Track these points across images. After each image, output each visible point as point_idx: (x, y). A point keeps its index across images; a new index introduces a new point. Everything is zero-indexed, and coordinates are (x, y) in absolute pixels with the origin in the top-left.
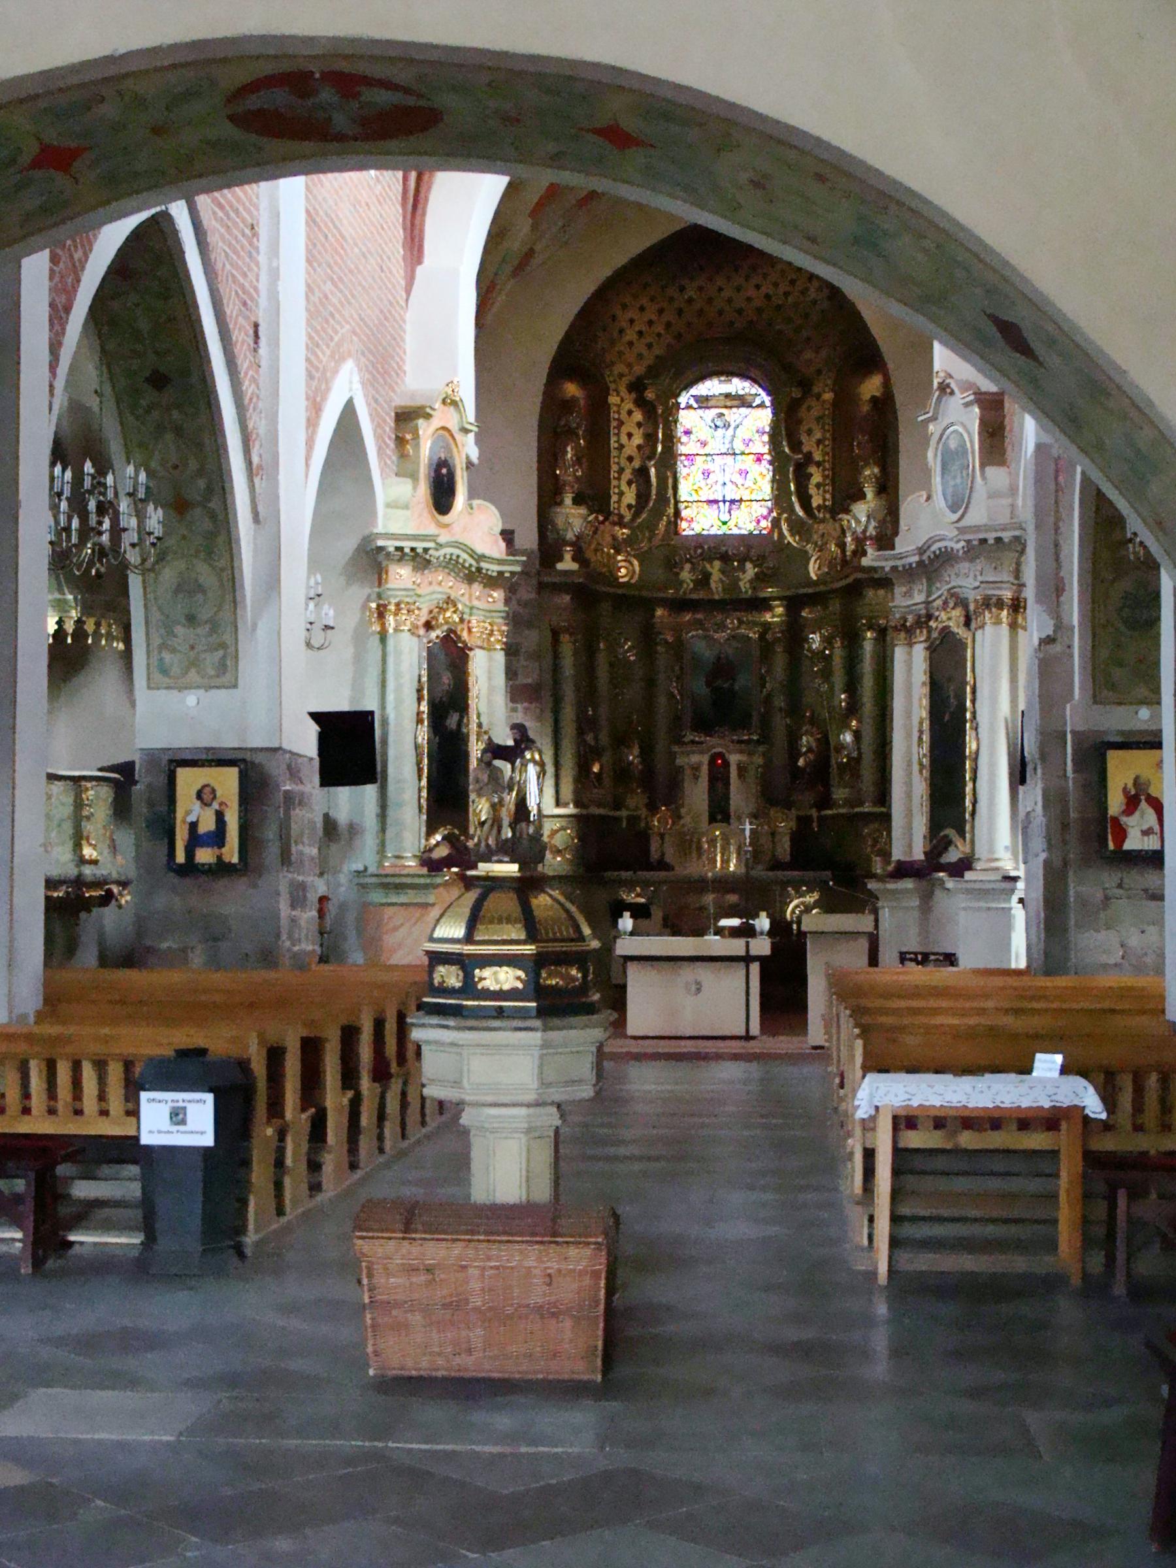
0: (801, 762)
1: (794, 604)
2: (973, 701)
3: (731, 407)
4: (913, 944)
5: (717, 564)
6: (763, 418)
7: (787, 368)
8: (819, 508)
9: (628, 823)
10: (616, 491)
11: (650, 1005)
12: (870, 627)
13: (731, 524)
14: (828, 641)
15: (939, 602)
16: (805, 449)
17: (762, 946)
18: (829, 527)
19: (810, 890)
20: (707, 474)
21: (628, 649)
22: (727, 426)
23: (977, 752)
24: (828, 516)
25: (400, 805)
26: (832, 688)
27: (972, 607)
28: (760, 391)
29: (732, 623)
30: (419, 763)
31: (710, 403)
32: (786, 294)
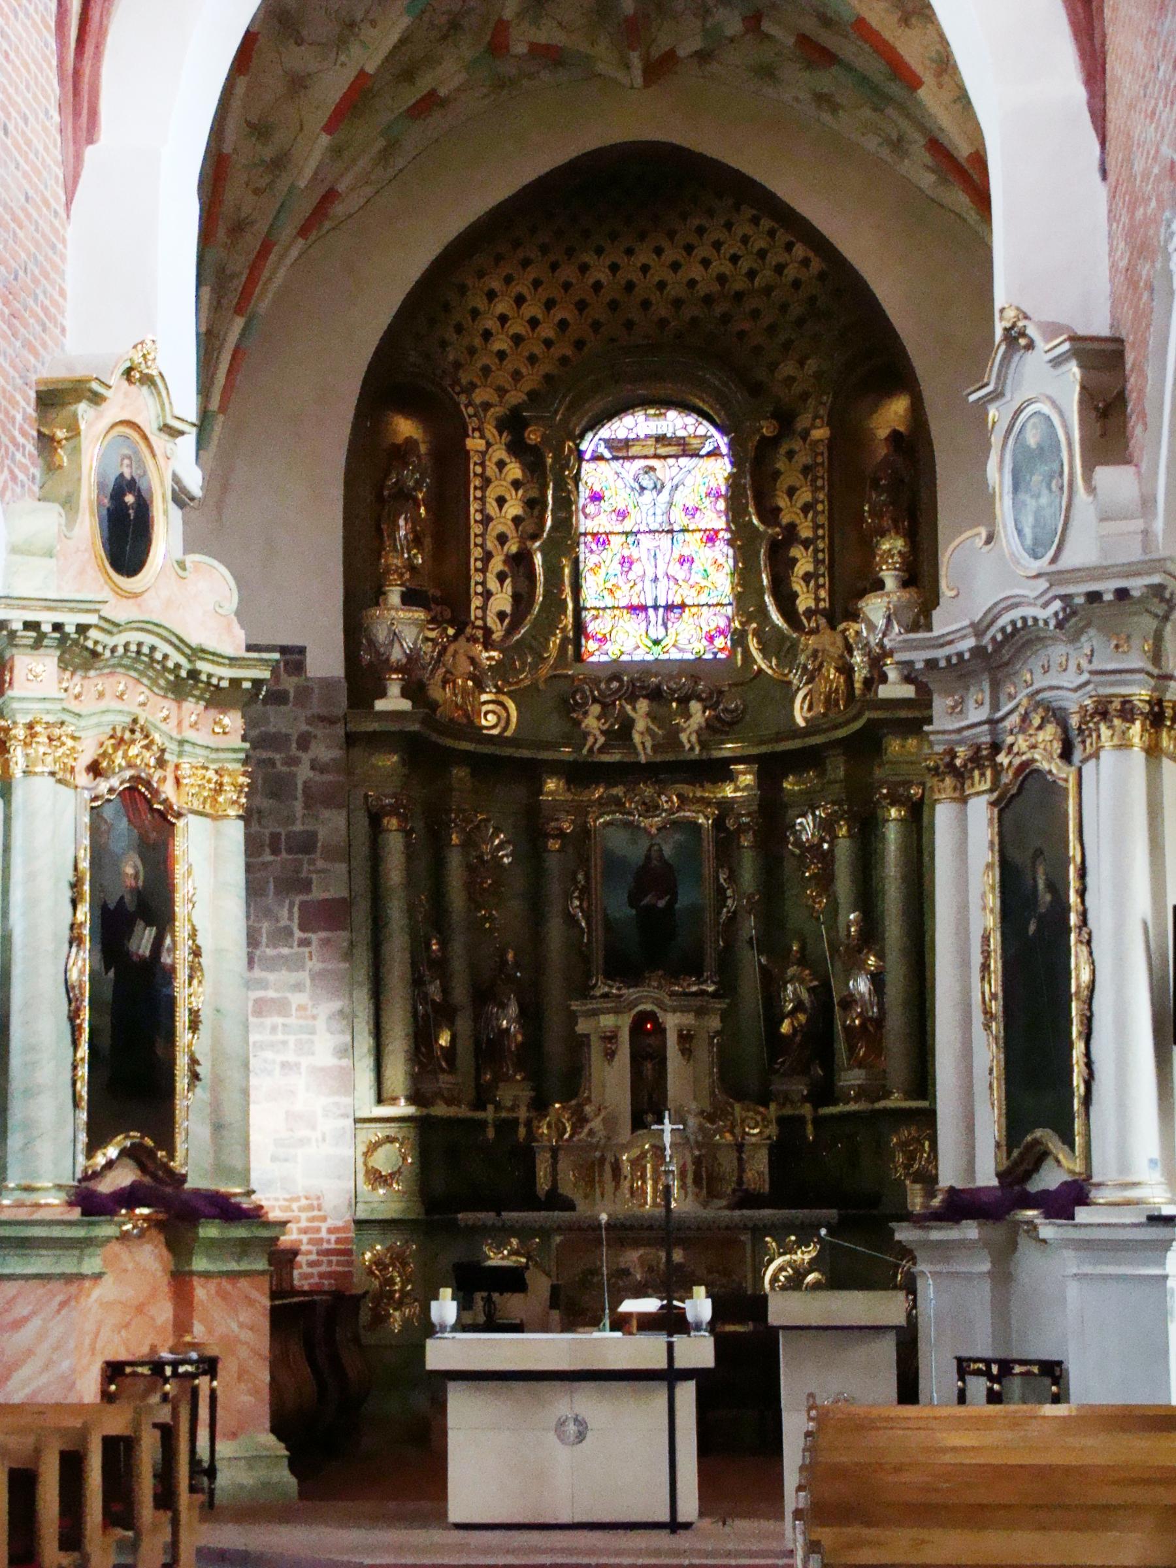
0: (785, 1027)
1: (771, 769)
2: (1082, 893)
3: (665, 457)
4: (982, 1346)
5: (643, 705)
6: (719, 471)
7: (756, 390)
8: (809, 613)
9: (497, 1132)
10: (479, 589)
11: (488, 1461)
13: (668, 641)
14: (827, 826)
15: (1015, 719)
16: (785, 519)
17: (698, 1351)
18: (827, 641)
19: (802, 1242)
20: (627, 562)
21: (501, 847)
22: (658, 488)
23: (1092, 987)
24: (823, 622)
25: (30, 1093)
27: (1074, 721)
28: (712, 431)
29: (670, 800)
30: (73, 1016)
31: (633, 451)
32: (752, 274)
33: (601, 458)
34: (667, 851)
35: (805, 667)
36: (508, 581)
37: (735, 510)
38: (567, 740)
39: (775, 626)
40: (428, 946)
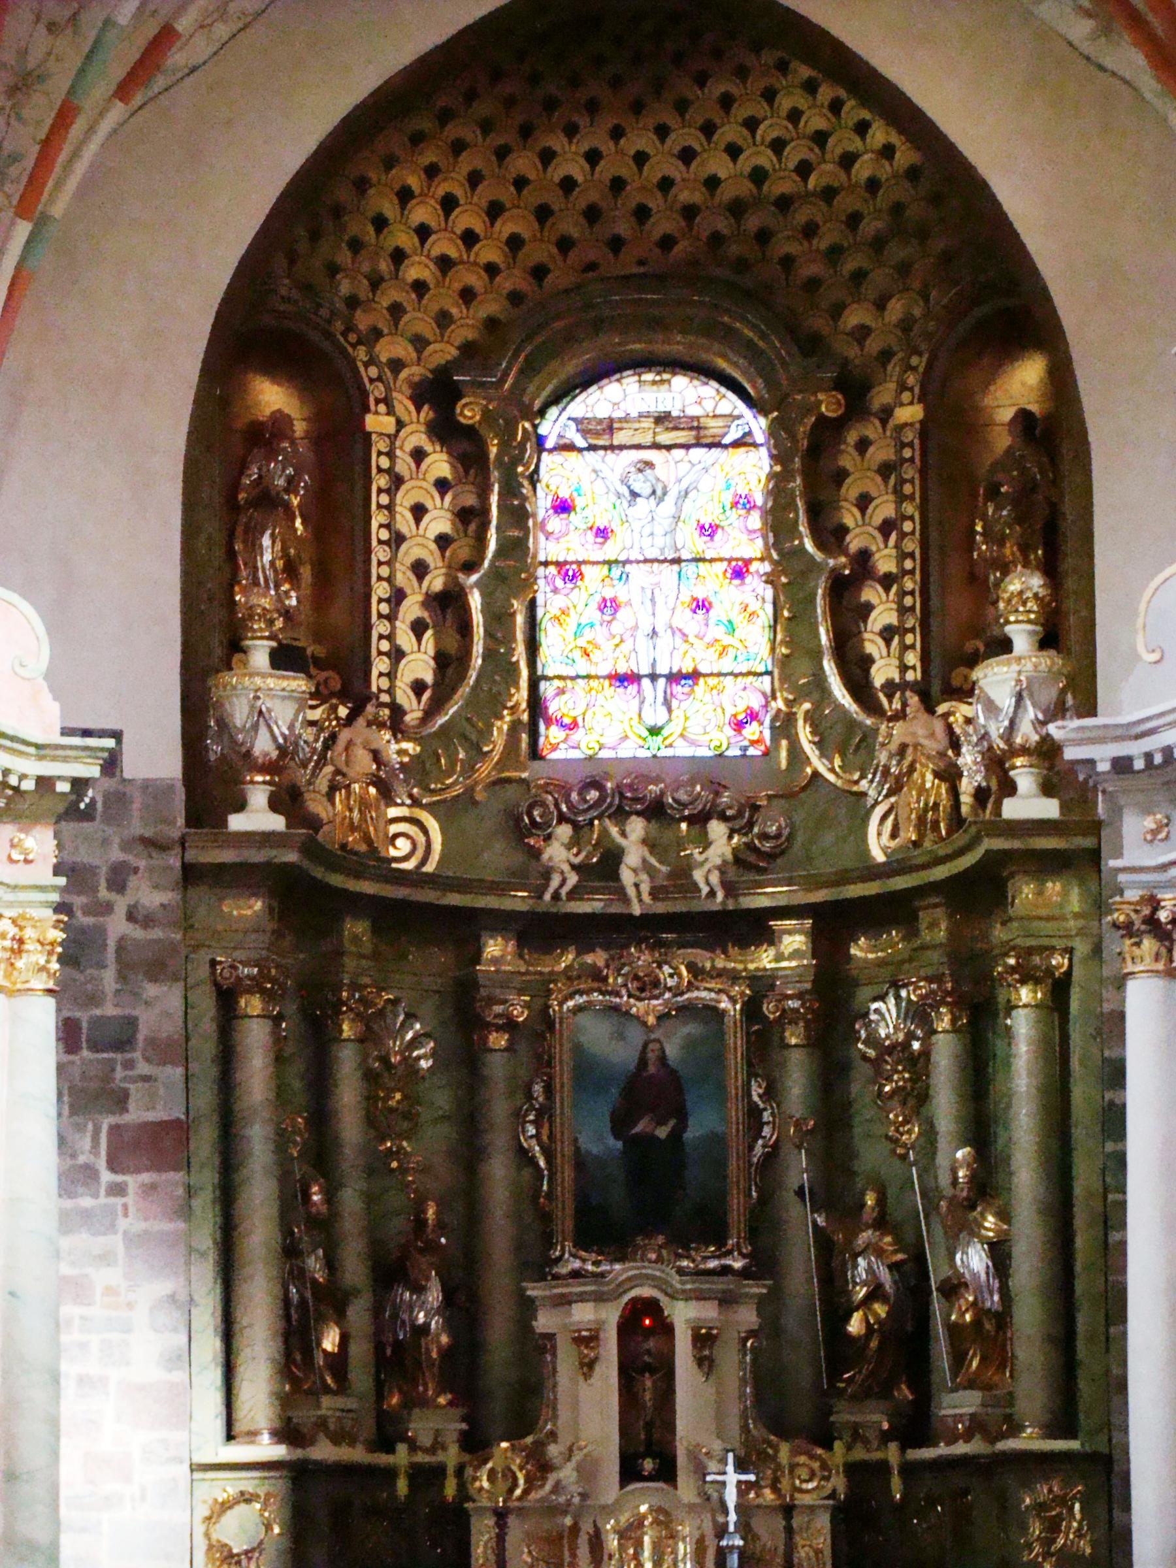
0: (855, 1325)
1: (833, 925)
3: (668, 448)
5: (637, 827)
6: (753, 470)
7: (811, 346)
8: (890, 688)
9: (411, 1486)
10: (385, 646)
12: (1027, 976)
14: (919, 1014)
16: (854, 543)
18: (918, 730)
21: (416, 1043)
22: (658, 494)
24: (914, 700)
26: (930, 1133)
28: (741, 407)
29: (676, 973)
31: (619, 438)
32: (804, 169)
33: (570, 447)
34: (672, 1051)
35: (886, 772)
36: (429, 633)
37: (778, 525)
38: (516, 879)
39: (839, 707)
40: (307, 1196)
